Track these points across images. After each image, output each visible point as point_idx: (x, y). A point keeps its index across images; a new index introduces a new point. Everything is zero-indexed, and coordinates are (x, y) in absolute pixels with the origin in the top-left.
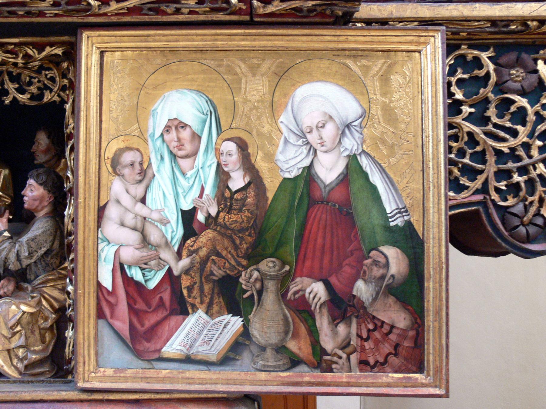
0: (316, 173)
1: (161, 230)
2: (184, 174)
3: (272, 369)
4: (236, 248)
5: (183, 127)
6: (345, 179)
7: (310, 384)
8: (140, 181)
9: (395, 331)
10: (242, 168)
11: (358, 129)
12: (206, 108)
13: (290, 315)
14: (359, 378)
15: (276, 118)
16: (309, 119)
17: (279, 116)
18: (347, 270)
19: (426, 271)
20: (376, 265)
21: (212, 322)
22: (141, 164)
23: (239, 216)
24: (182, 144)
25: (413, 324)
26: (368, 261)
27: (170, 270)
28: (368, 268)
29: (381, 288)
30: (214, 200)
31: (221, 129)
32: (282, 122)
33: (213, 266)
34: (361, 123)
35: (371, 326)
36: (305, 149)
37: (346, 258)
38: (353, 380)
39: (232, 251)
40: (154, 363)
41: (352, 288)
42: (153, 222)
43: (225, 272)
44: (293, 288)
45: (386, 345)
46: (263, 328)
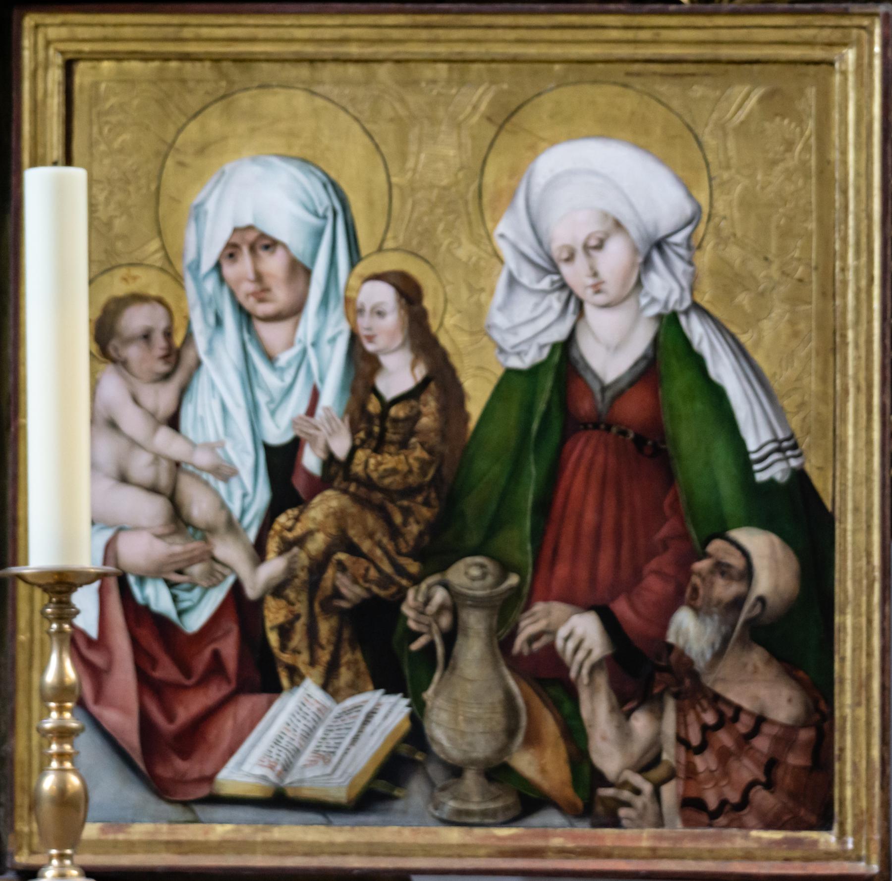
0: (582, 357)
1: (216, 493)
2: (270, 359)
3: (476, 820)
4: (395, 533)
5: (267, 247)
6: (648, 371)
7: (563, 852)
8: (166, 377)
9: (766, 729)
10: (408, 345)
11: (682, 251)
12: (323, 200)
13: (521, 689)
14: (680, 838)
15: (489, 225)
16: (567, 227)
17: (496, 221)
18: (655, 586)
19: (837, 589)
20: (723, 574)
21: (337, 709)
22: (168, 334)
23: (402, 457)
24: (263, 288)
25: (808, 712)
26: (702, 565)
27: (237, 588)
28: (703, 580)
29: (733, 627)
30: (343, 420)
31: (358, 251)
32: (502, 236)
33: (339, 575)
34: (689, 238)
35: (710, 718)
36: (555, 302)
37: (651, 555)
38: (665, 844)
39: (385, 540)
40: (198, 809)
41: (665, 627)
42: (197, 472)
43: (368, 590)
44: (528, 627)
45: (746, 762)
46: (456, 722)
